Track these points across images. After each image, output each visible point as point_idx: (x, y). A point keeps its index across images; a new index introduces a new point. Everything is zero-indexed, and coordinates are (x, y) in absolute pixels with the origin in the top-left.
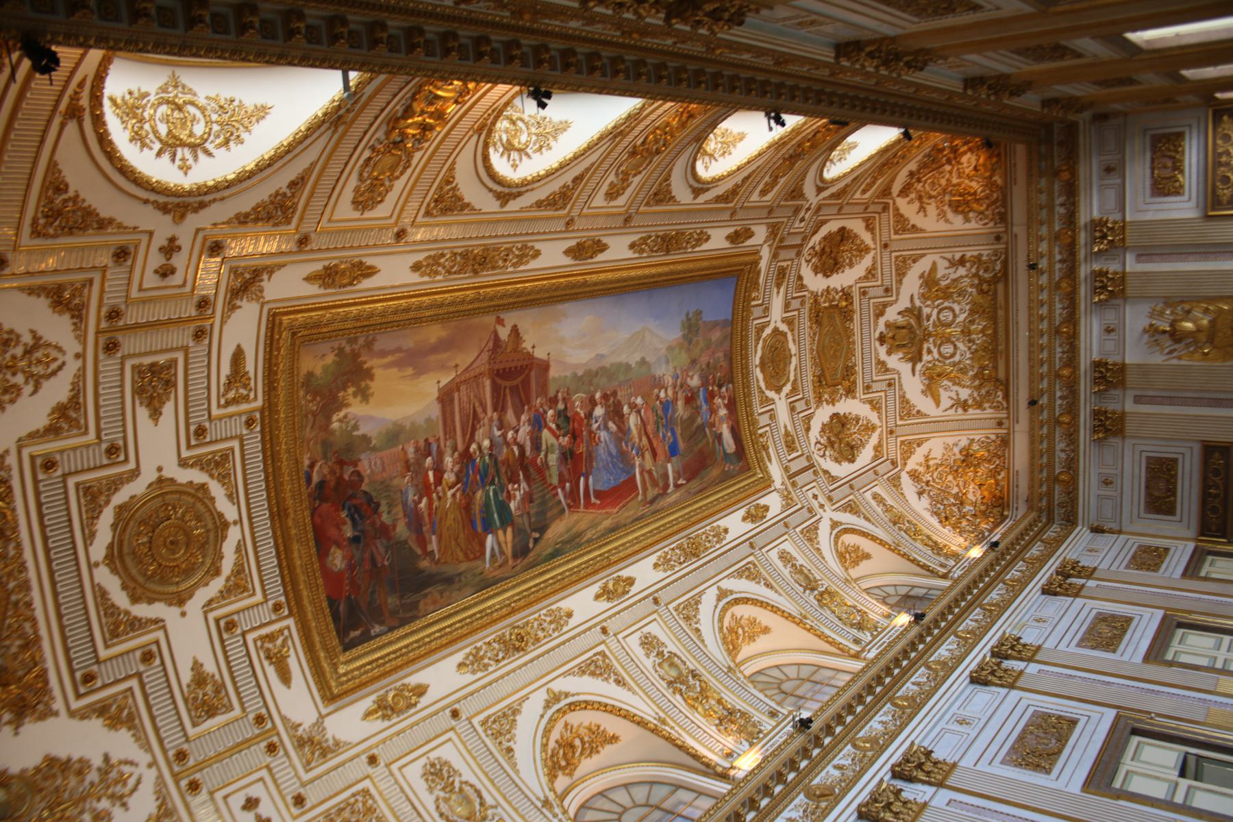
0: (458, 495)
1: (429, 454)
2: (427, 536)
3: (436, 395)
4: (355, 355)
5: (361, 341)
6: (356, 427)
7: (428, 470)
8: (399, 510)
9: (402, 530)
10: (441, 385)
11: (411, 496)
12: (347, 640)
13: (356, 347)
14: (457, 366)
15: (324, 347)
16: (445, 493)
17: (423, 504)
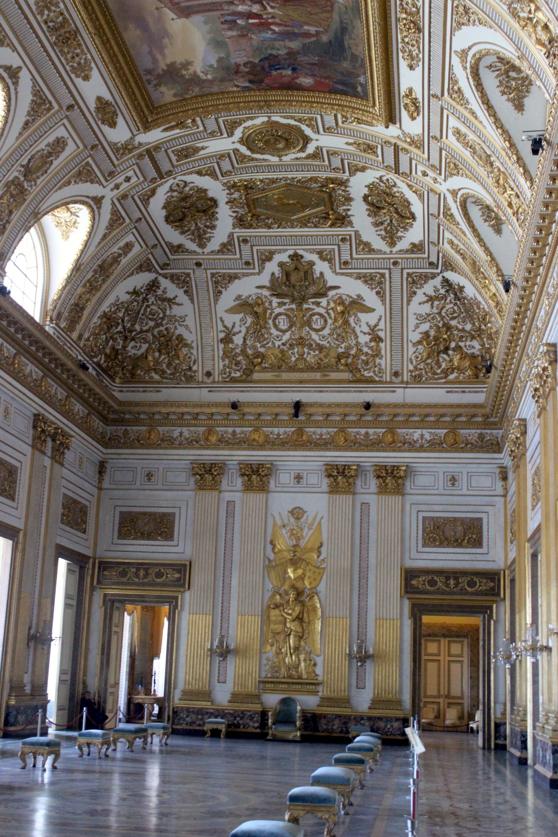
0: (272, 4)
1: (235, 21)
2: (302, 31)
3: (184, 20)
4: (159, 76)
5: (149, 77)
6: (211, 66)
7: (247, 23)
8: (277, 44)
9: (294, 45)
10: (175, 17)
11: (269, 35)
12: (362, 94)
13: (152, 78)
14: (157, 9)
15: (155, 95)
16: (270, 13)
17: (277, 29)
